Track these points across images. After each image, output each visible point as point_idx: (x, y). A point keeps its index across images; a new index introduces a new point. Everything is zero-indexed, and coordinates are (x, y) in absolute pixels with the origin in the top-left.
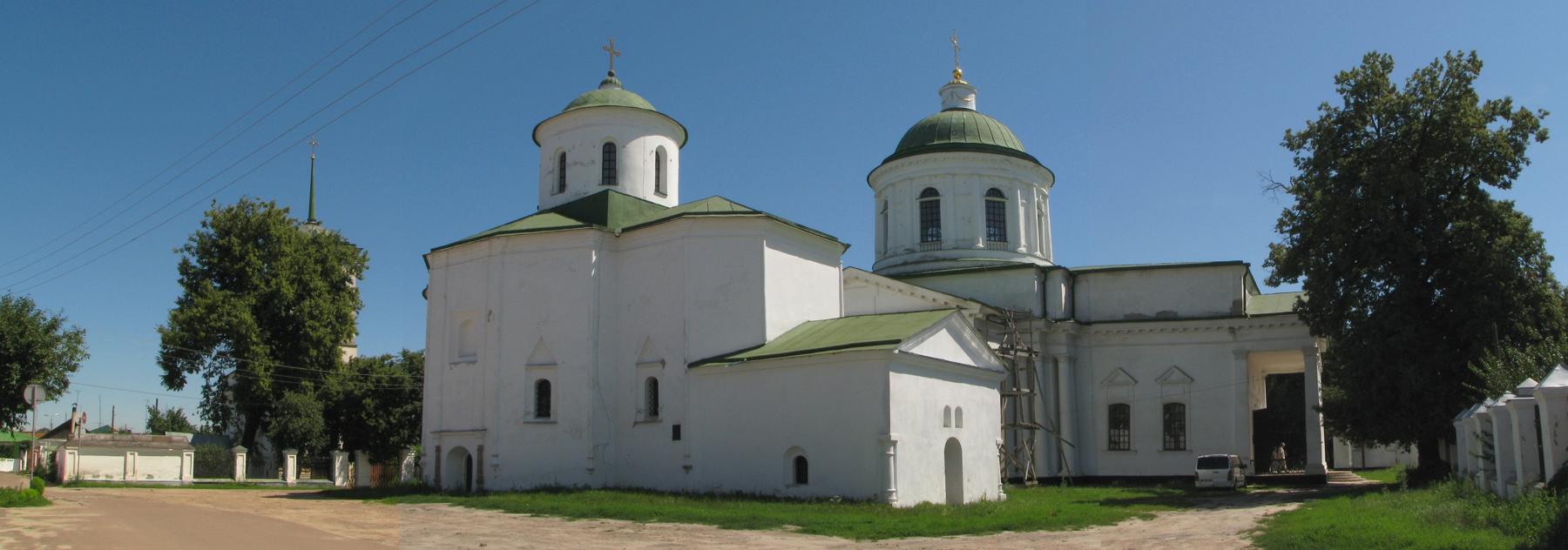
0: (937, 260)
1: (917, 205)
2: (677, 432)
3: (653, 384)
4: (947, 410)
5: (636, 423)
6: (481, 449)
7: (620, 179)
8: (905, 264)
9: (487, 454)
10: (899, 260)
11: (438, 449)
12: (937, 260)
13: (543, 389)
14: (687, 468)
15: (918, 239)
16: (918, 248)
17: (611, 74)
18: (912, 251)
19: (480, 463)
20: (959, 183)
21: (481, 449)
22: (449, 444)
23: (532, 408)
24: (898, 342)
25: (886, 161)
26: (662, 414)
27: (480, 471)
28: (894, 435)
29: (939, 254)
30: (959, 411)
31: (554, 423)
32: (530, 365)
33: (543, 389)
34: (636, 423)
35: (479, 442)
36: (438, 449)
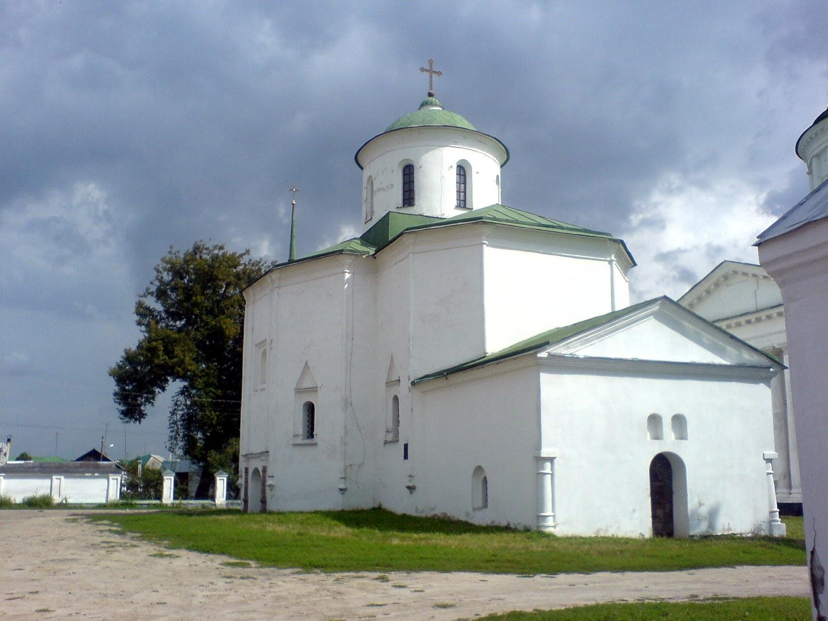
4: (654, 420)
5: (386, 442)
6: (264, 470)
7: (416, 202)
9: (269, 473)
11: (247, 469)
14: (411, 489)
17: (430, 95)
23: (300, 429)
27: (264, 491)
28: (545, 452)
30: (679, 421)
31: (316, 444)
32: (299, 391)
33: (310, 409)
34: (386, 442)
35: (263, 464)
36: (247, 469)
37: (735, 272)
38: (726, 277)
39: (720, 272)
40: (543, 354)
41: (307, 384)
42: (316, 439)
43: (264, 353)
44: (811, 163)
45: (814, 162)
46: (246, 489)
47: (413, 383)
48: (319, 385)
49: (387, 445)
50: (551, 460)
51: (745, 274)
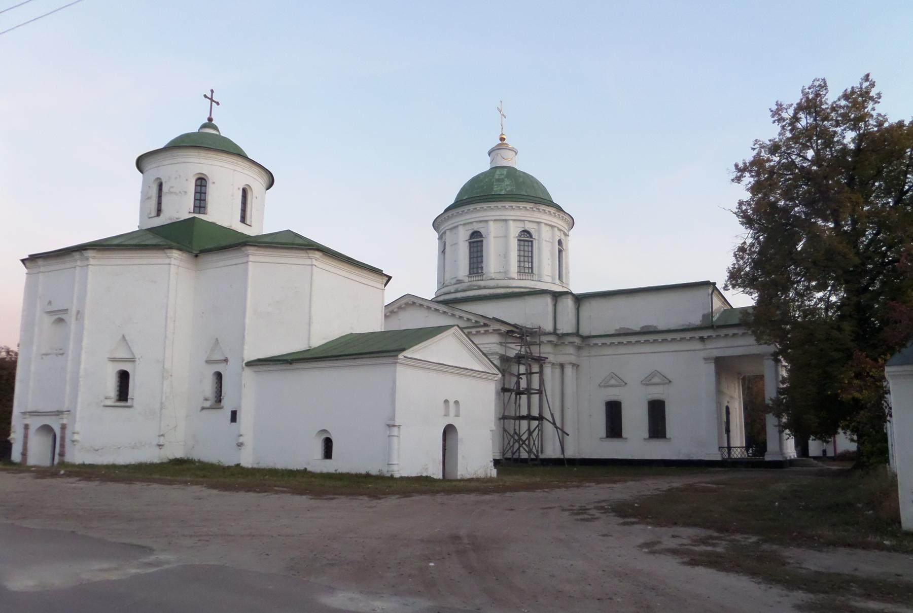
0: (480, 288)
1: (467, 244)
2: (234, 416)
3: (219, 376)
4: (446, 401)
5: (203, 408)
6: (63, 427)
8: (456, 291)
10: (452, 289)
11: (26, 427)
12: (480, 288)
13: (124, 377)
14: (240, 445)
15: (467, 273)
16: (467, 279)
18: (460, 282)
19: (63, 439)
20: (501, 227)
21: (63, 427)
22: (35, 423)
24: (403, 350)
25: (446, 211)
26: (224, 402)
27: (62, 446)
29: (482, 283)
36: (26, 427)
37: (414, 303)
38: (407, 304)
39: (405, 301)
40: (401, 356)
41: (123, 354)
42: (129, 403)
43: (60, 320)
44: (445, 233)
45: (448, 232)
46: (25, 444)
47: (250, 364)
48: (137, 356)
49: (204, 412)
50: (399, 427)
51: (421, 305)
